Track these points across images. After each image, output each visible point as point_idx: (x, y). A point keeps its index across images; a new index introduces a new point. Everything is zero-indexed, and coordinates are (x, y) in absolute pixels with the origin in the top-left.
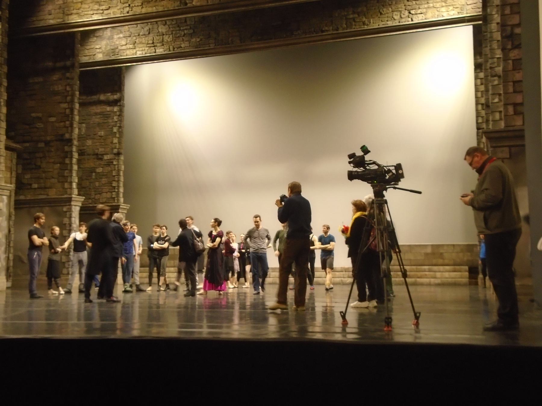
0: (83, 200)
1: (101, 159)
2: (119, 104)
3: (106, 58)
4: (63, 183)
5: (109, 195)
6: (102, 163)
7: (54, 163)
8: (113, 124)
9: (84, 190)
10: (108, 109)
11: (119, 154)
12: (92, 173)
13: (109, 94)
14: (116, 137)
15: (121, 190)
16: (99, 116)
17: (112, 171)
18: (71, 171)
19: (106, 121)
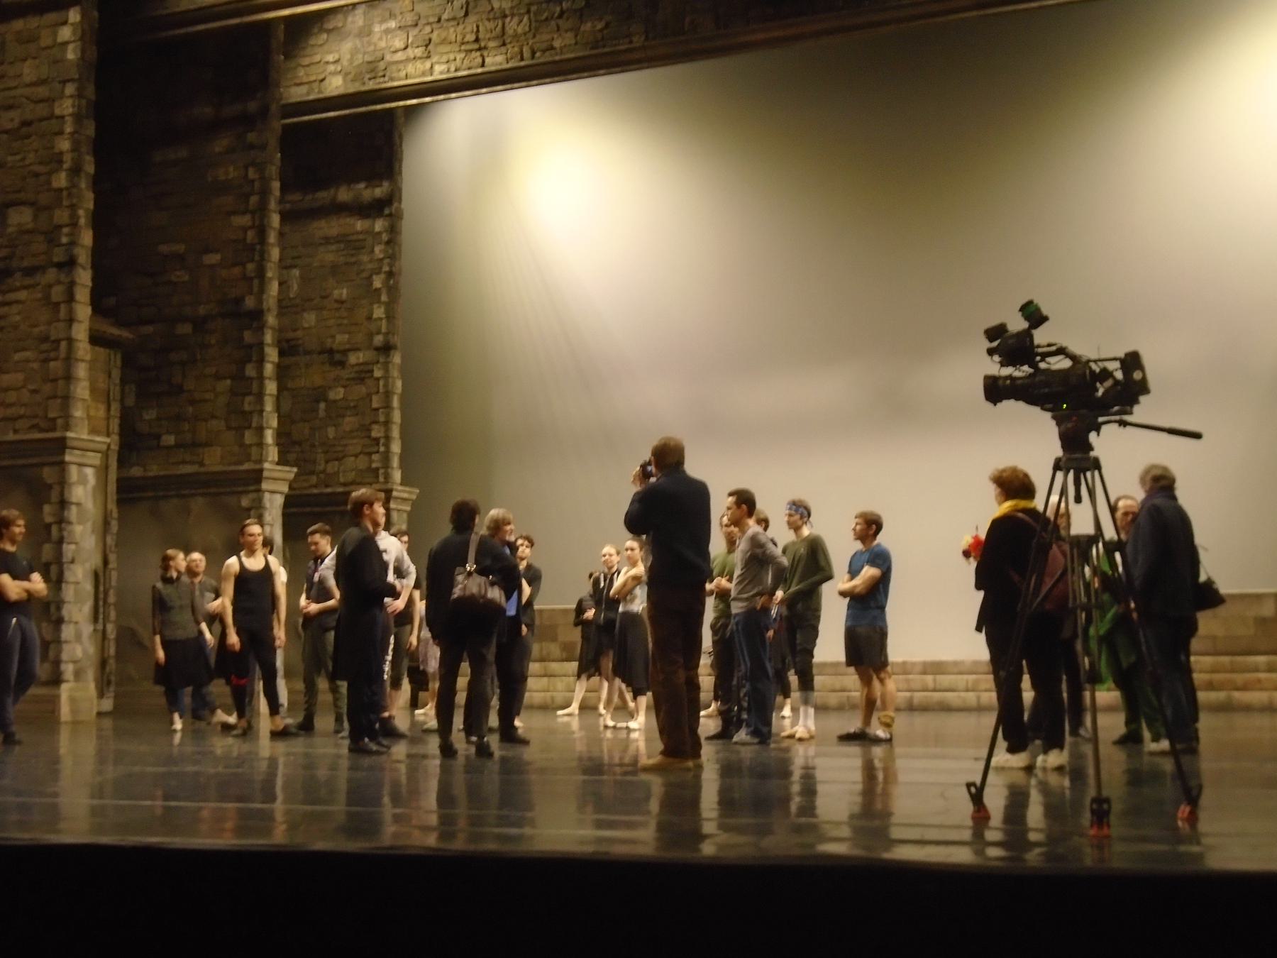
0: (292, 476)
1: (342, 364)
2: (387, 211)
3: (353, 88)
4: (240, 430)
5: (362, 462)
6: (345, 374)
7: (218, 377)
8: (370, 266)
9: (297, 448)
10: (360, 225)
11: (387, 349)
12: (318, 402)
13: (362, 185)
14: (379, 302)
15: (396, 448)
16: (333, 247)
17: (369, 395)
18: (260, 396)
19: (353, 260)
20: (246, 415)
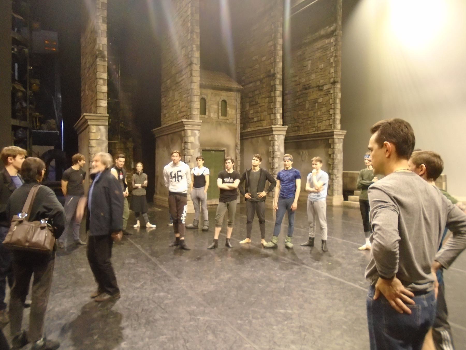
0: (286, 129)
1: (322, 90)
2: (334, 34)
4: (270, 114)
5: (327, 123)
6: (322, 93)
7: (265, 98)
8: (330, 55)
9: (310, 119)
10: (327, 41)
11: (334, 83)
12: (315, 103)
13: (327, 27)
14: (332, 67)
15: (338, 117)
16: (319, 51)
17: (329, 99)
19: (324, 54)
20: (271, 109)
